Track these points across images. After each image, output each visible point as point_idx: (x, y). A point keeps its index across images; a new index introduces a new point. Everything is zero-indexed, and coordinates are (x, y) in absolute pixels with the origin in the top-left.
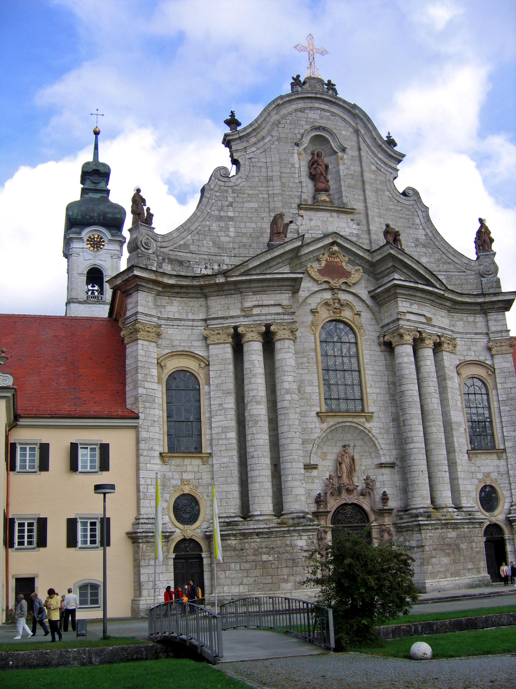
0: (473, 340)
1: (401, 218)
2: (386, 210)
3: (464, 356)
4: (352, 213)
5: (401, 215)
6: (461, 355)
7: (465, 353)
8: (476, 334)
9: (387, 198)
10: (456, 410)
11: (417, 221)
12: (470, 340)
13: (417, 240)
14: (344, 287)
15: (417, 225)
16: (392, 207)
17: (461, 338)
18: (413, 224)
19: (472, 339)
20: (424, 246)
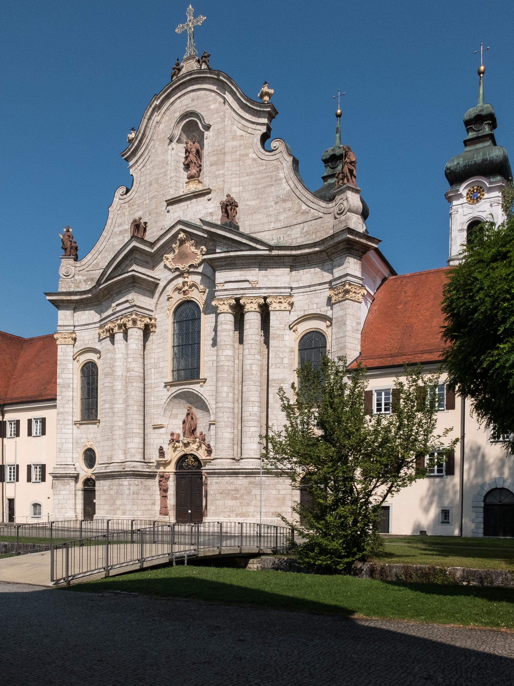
0: (317, 292)
1: (263, 178)
2: (247, 176)
3: (304, 311)
4: (209, 193)
5: (264, 175)
6: (301, 311)
7: (306, 308)
8: (320, 284)
9: (250, 162)
10: (279, 367)
11: (282, 175)
12: (314, 292)
13: (278, 197)
14: (192, 270)
15: (280, 179)
16: (255, 170)
17: (304, 292)
18: (276, 181)
19: (316, 290)
20: (284, 201)
